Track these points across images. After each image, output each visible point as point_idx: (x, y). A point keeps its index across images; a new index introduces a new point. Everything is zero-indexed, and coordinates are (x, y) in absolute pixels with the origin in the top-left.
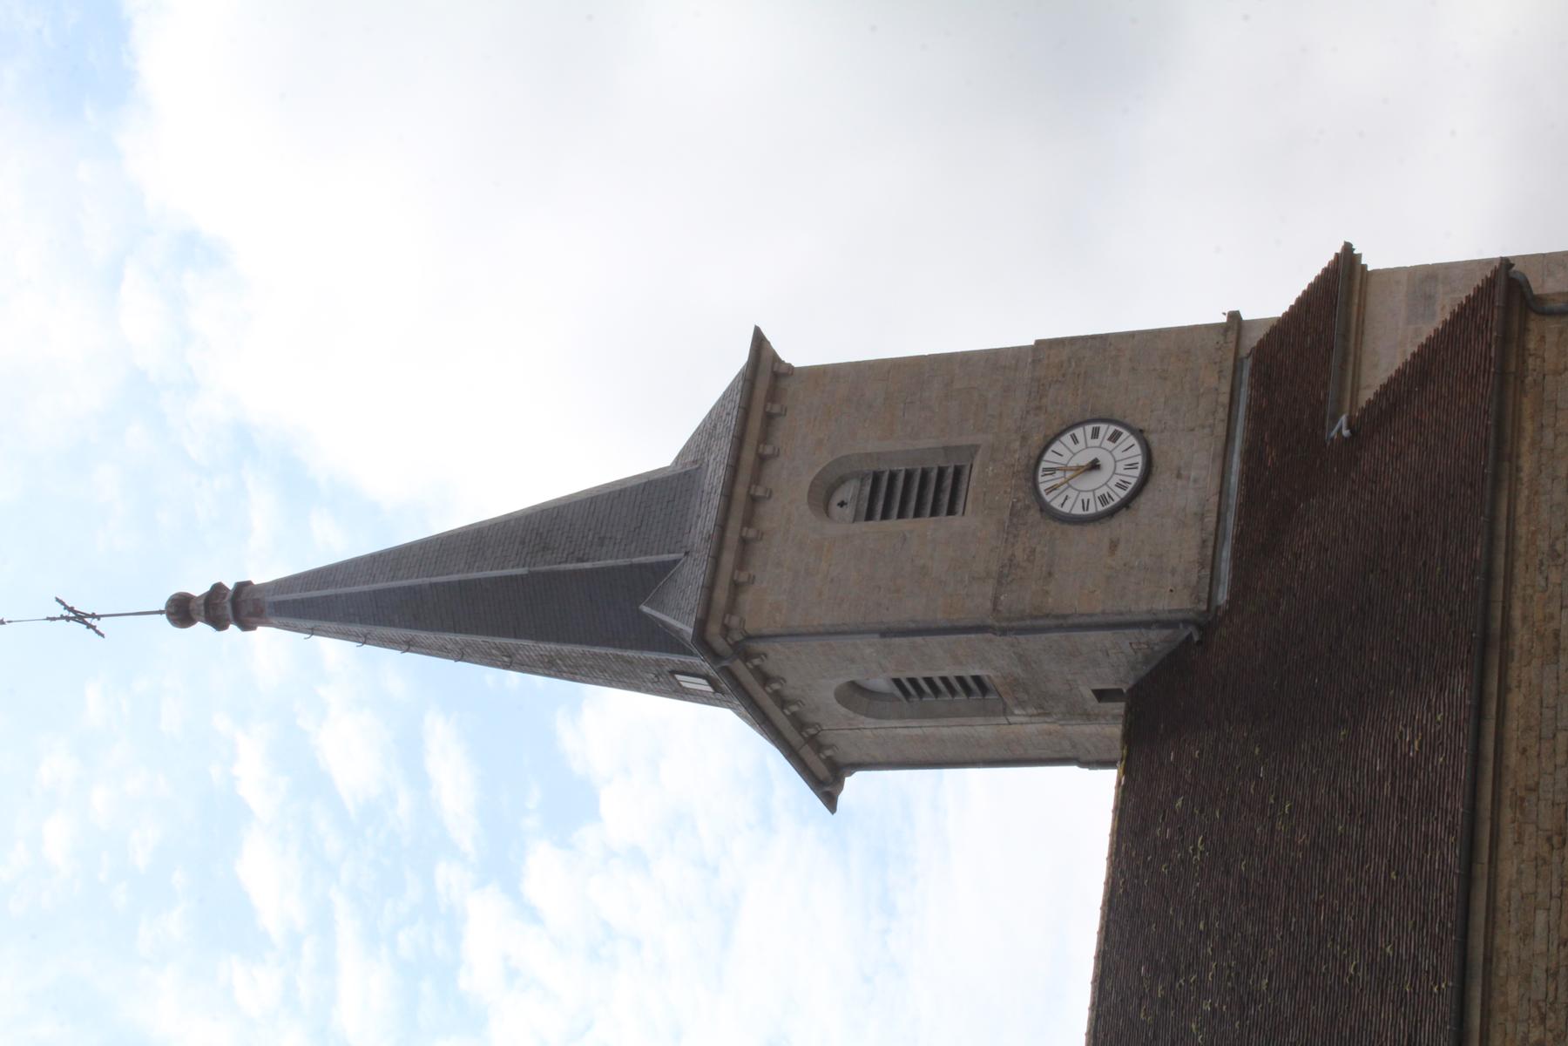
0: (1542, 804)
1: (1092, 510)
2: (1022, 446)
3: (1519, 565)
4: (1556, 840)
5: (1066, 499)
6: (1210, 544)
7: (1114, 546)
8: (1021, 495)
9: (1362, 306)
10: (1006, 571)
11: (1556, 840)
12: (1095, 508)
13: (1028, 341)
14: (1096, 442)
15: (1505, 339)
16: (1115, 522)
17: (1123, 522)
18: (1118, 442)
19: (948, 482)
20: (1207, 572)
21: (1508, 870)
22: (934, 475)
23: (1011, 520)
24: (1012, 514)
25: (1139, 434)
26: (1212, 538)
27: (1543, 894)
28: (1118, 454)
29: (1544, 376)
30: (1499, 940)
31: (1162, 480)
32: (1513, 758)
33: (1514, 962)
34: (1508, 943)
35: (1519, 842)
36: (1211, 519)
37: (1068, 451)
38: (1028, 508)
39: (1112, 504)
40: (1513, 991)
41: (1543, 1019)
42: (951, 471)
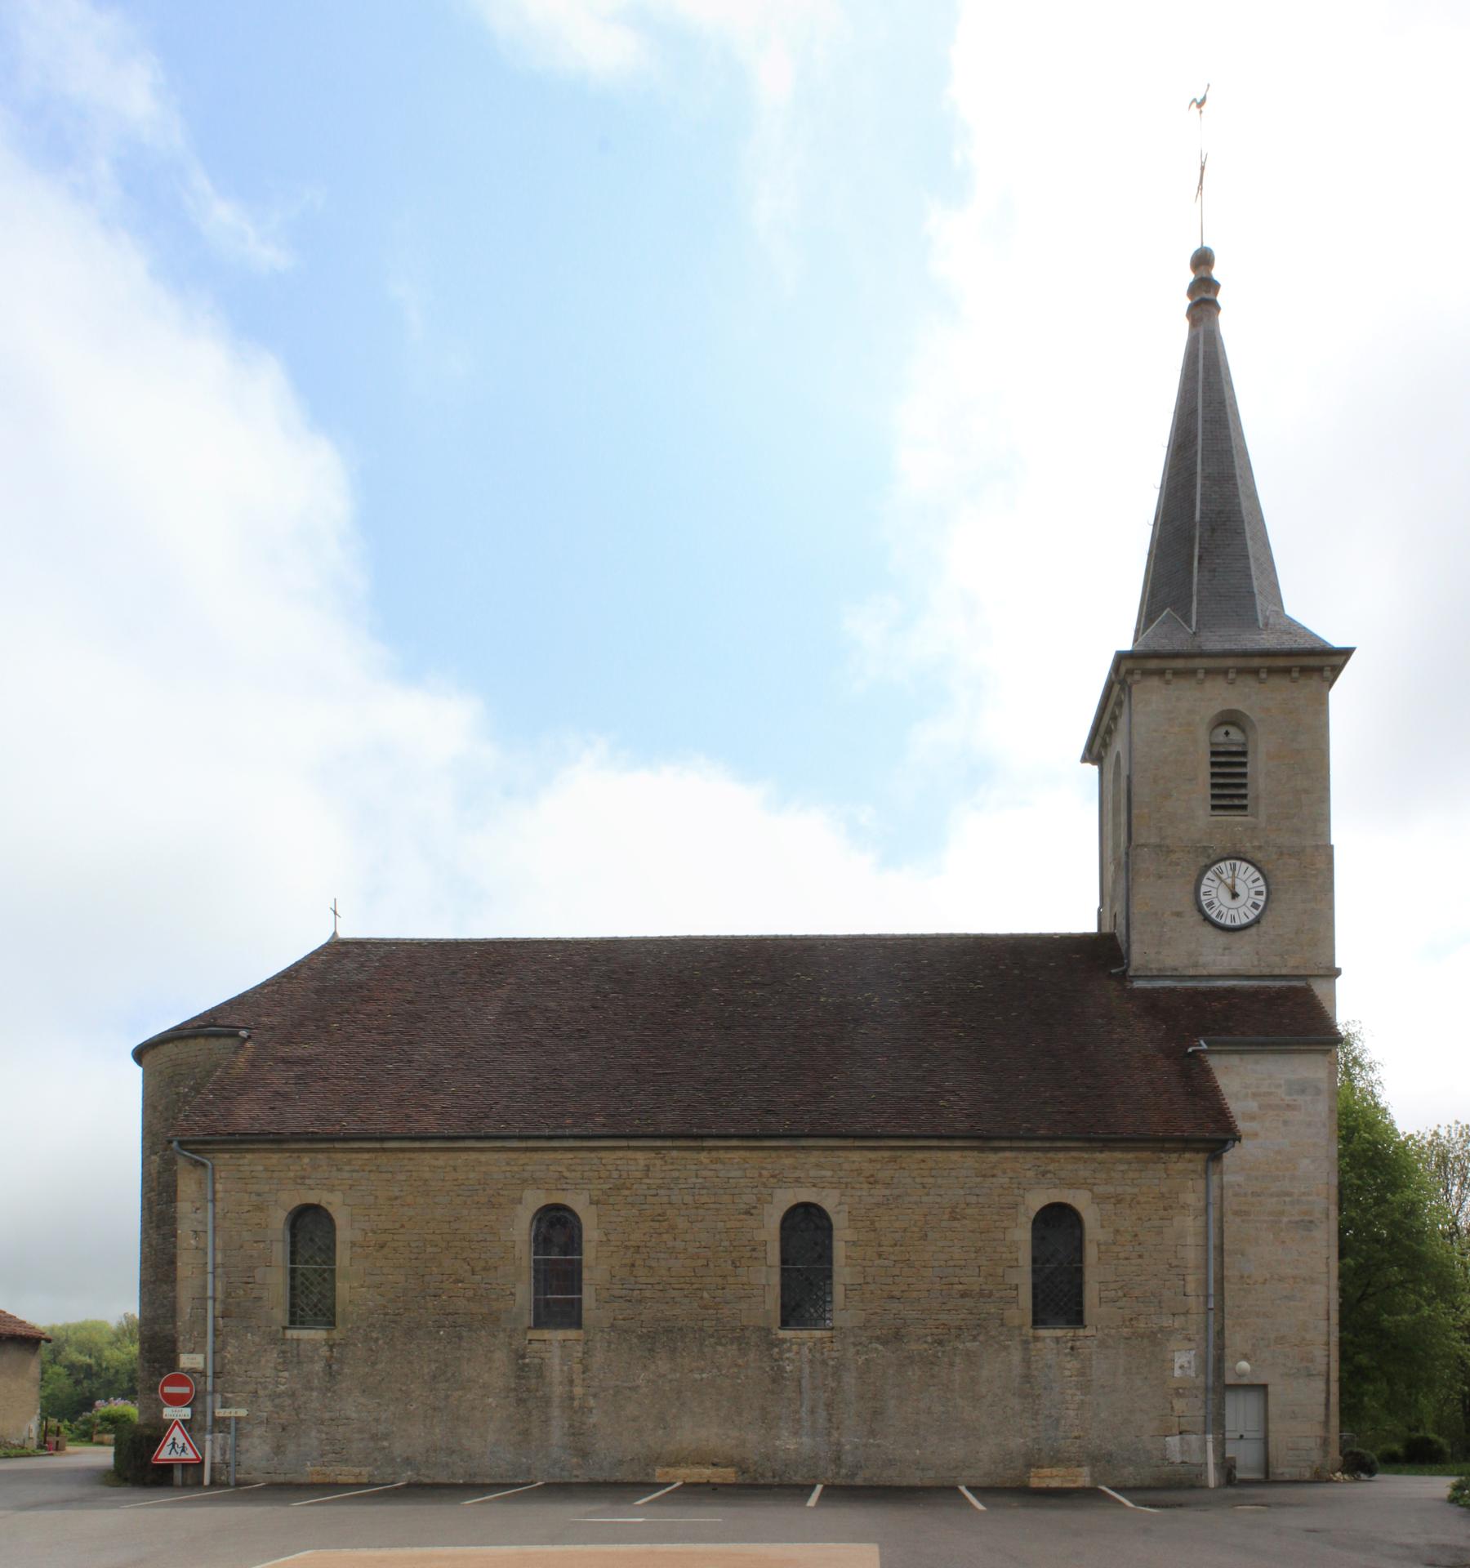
0: (893, 1172)
1: (1203, 898)
2: (1253, 847)
3: (1040, 1154)
4: (872, 1179)
5: (1213, 881)
6: (1175, 973)
7: (1178, 914)
8: (1218, 851)
9: (1301, 1052)
10: (1164, 849)
11: (872, 1179)
13: (1333, 842)
14: (1252, 893)
15: (1186, 1140)
16: (1196, 913)
17: (1194, 917)
18: (1252, 909)
19: (1236, 802)
20: (1155, 973)
21: (856, 1156)
22: (1243, 791)
23: (1200, 847)
24: (1204, 847)
25: (1257, 921)
26: (1178, 974)
27: (841, 1174)
28: (1241, 911)
29: (1164, 1163)
30: (816, 1153)
31: (1223, 939)
32: (919, 1155)
33: (804, 1161)
34: (814, 1157)
35: (871, 1161)
36: (1191, 972)
37: (1247, 879)
38: (1209, 857)
39: (1207, 910)
40: (788, 1161)
41: (773, 1176)
42: (1244, 802)
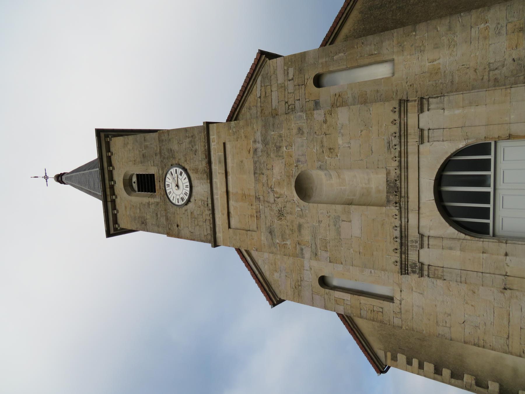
5: (174, 198)
12: (181, 203)
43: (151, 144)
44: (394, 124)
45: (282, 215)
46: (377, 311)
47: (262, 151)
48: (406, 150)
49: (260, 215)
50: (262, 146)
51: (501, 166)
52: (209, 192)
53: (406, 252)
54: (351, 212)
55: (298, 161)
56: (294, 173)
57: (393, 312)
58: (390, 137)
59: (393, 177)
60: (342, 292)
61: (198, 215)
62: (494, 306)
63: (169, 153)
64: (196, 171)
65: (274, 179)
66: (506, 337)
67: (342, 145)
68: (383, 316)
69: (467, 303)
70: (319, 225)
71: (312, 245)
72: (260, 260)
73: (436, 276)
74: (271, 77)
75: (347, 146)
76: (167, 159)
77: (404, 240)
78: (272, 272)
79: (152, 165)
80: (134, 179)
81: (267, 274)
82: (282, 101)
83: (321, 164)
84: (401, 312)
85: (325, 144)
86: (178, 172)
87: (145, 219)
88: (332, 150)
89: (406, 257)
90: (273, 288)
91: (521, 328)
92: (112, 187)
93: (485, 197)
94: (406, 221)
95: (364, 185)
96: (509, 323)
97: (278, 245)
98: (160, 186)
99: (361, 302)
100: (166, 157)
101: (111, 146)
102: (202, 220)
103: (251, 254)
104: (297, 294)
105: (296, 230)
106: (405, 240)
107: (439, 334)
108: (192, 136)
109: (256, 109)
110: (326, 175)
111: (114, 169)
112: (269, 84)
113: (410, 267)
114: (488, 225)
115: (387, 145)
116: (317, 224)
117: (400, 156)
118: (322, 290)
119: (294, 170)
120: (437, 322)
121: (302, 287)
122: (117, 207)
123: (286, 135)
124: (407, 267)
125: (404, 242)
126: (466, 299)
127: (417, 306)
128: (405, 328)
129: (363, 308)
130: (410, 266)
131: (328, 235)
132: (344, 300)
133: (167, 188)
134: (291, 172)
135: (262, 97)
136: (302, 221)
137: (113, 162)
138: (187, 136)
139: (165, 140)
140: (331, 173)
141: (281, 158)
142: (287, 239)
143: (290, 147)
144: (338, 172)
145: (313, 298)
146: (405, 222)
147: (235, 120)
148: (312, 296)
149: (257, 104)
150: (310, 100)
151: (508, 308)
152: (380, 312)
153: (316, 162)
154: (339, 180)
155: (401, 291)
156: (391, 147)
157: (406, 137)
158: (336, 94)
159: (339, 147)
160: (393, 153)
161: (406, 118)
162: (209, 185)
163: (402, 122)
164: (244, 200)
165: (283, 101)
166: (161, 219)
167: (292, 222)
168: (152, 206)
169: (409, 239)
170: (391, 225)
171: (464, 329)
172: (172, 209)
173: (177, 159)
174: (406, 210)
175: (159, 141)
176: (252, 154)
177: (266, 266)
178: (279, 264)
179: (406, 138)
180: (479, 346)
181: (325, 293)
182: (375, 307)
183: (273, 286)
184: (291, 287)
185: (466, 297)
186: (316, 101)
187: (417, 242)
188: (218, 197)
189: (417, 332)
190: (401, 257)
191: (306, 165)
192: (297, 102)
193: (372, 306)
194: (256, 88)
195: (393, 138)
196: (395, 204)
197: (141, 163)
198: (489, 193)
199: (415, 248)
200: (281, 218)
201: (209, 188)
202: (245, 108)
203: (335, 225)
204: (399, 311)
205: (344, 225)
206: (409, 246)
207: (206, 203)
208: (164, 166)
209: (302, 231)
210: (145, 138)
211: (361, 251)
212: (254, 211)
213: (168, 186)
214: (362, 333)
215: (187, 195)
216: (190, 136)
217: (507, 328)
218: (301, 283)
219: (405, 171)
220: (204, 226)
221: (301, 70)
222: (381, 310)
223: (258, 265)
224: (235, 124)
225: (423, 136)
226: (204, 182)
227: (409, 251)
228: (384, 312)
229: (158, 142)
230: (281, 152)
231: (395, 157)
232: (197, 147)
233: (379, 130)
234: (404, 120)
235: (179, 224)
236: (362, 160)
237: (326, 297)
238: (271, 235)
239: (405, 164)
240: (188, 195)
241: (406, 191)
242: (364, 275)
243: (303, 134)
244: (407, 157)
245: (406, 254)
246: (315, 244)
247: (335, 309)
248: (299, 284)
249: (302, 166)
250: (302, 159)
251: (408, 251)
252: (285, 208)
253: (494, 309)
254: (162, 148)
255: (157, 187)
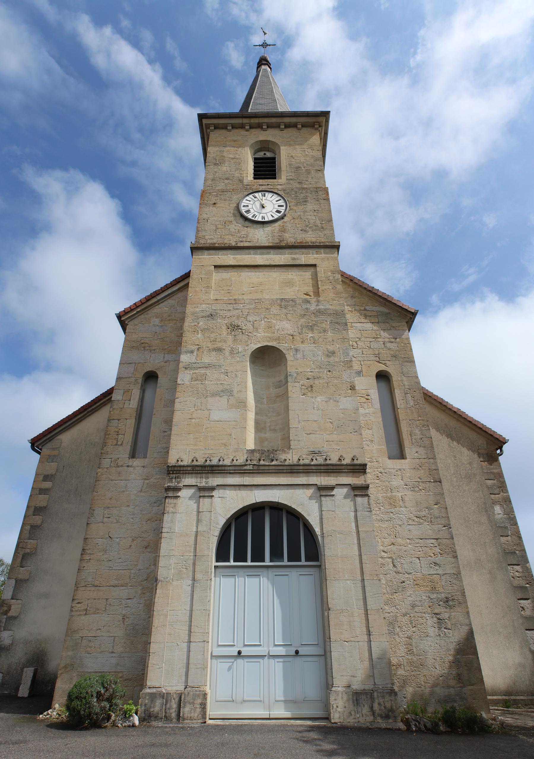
1: (242, 208)
5: (249, 201)
12: (243, 210)
43: (312, 178)
44: (340, 458)
45: (233, 330)
46: (118, 438)
47: (307, 309)
48: (312, 471)
49: (232, 304)
50: (314, 309)
51: (294, 574)
52: (257, 245)
53: (194, 472)
54: (239, 410)
55: (297, 350)
56: (282, 345)
57: (118, 458)
58: (326, 454)
59: (281, 457)
60: (139, 398)
61: (229, 229)
62: (131, 569)
63: (302, 199)
64: (283, 230)
65: (275, 321)
66: (96, 583)
67: (315, 401)
68: (112, 445)
69: (133, 540)
70: (222, 373)
71: (197, 364)
72: (174, 302)
73: (168, 505)
74: (387, 323)
75: (315, 406)
76: (295, 196)
77: (208, 469)
78: (159, 315)
79: (288, 178)
80: (269, 155)
81: (157, 310)
82: (361, 334)
83: (294, 377)
84: (118, 467)
85: (316, 382)
86: (280, 209)
87: (221, 164)
88: (310, 389)
89: (188, 472)
90: (140, 317)
91: (107, 599)
92: (259, 126)
93: (258, 556)
94: (231, 471)
95: (269, 424)
96: (113, 586)
97: (196, 324)
98: (263, 185)
99: (128, 420)
100: (298, 194)
101: (309, 129)
102: (223, 234)
103: (181, 291)
104: (134, 345)
105: (216, 346)
106: (209, 470)
107: (94, 510)
108: (323, 228)
109: (352, 304)
110: (280, 381)
111: (281, 130)
112: (380, 321)
113: (177, 476)
114: (228, 561)
115: (316, 450)
116: (223, 371)
117: (304, 465)
118: (140, 376)
119: (286, 345)
120: (108, 508)
121: (144, 351)
122: (235, 131)
123: (326, 337)
124: (176, 473)
125: (206, 469)
126: (138, 539)
127: (127, 485)
128: (99, 472)
129: (121, 423)
130: (178, 477)
131: (211, 383)
132: (130, 400)
133: (260, 194)
134: (284, 342)
135: (366, 312)
136: (227, 353)
137: (290, 130)
138: (323, 221)
139: (318, 195)
140: (281, 388)
141: (300, 331)
142: (203, 335)
143: (312, 341)
144: (284, 395)
145: (130, 363)
146: (230, 470)
147: (342, 281)
148: (133, 363)
149: (358, 306)
150: (362, 365)
151: (130, 585)
152: (117, 442)
153: (296, 371)
154: (274, 396)
155: (144, 467)
156: (314, 455)
157: (326, 471)
158: (369, 395)
159: (314, 398)
160: (308, 456)
161: (347, 471)
162: (267, 245)
163: (343, 467)
164: (249, 285)
165: (361, 336)
166: (222, 184)
167: (225, 341)
168: (238, 173)
169: (209, 474)
170: (225, 454)
171: (102, 538)
172: (235, 197)
173: (295, 208)
174: (243, 471)
175: (317, 188)
176: (304, 297)
177: (167, 309)
178: (170, 325)
179: (324, 471)
180: (82, 554)
181: (137, 379)
182: (123, 436)
183: (142, 316)
184: (142, 339)
185: (141, 539)
186: (361, 372)
187: (206, 484)
188: (252, 254)
189: (95, 485)
190: (187, 466)
191: (292, 359)
192: (360, 351)
193: (123, 433)
194: (376, 305)
195: (324, 457)
196: (249, 458)
197: (290, 165)
198: (263, 561)
199: (199, 481)
200: (229, 329)
201: (262, 245)
202: (353, 292)
203: (222, 391)
204: (118, 465)
205: (223, 401)
206: (202, 475)
207: (244, 240)
208: (286, 192)
209: (214, 353)
210: (319, 171)
211: (193, 420)
212: (236, 298)
213: (263, 195)
214: (81, 421)
215: (253, 217)
216: (323, 225)
217: (107, 584)
218: (147, 350)
219: (289, 470)
220: (216, 236)
221: (395, 357)
222: (119, 443)
223: (167, 299)
224: (338, 279)
225: (328, 490)
226: (269, 239)
227: (196, 475)
228: (117, 446)
229: (315, 186)
230: (307, 331)
231: (303, 460)
232: (310, 233)
233: (333, 441)
234: (345, 469)
235: (217, 205)
236: (299, 422)
237: (133, 380)
238: (208, 316)
239: (296, 470)
240: (253, 219)
241: (265, 471)
242: (162, 422)
243: (328, 356)
244: (303, 472)
245: (192, 472)
246: (200, 368)
247: (118, 389)
248: (147, 348)
249: (292, 354)
250: (299, 356)
251: (195, 473)
252: (241, 333)
253: (128, 569)
254: (309, 191)
255: (261, 181)
